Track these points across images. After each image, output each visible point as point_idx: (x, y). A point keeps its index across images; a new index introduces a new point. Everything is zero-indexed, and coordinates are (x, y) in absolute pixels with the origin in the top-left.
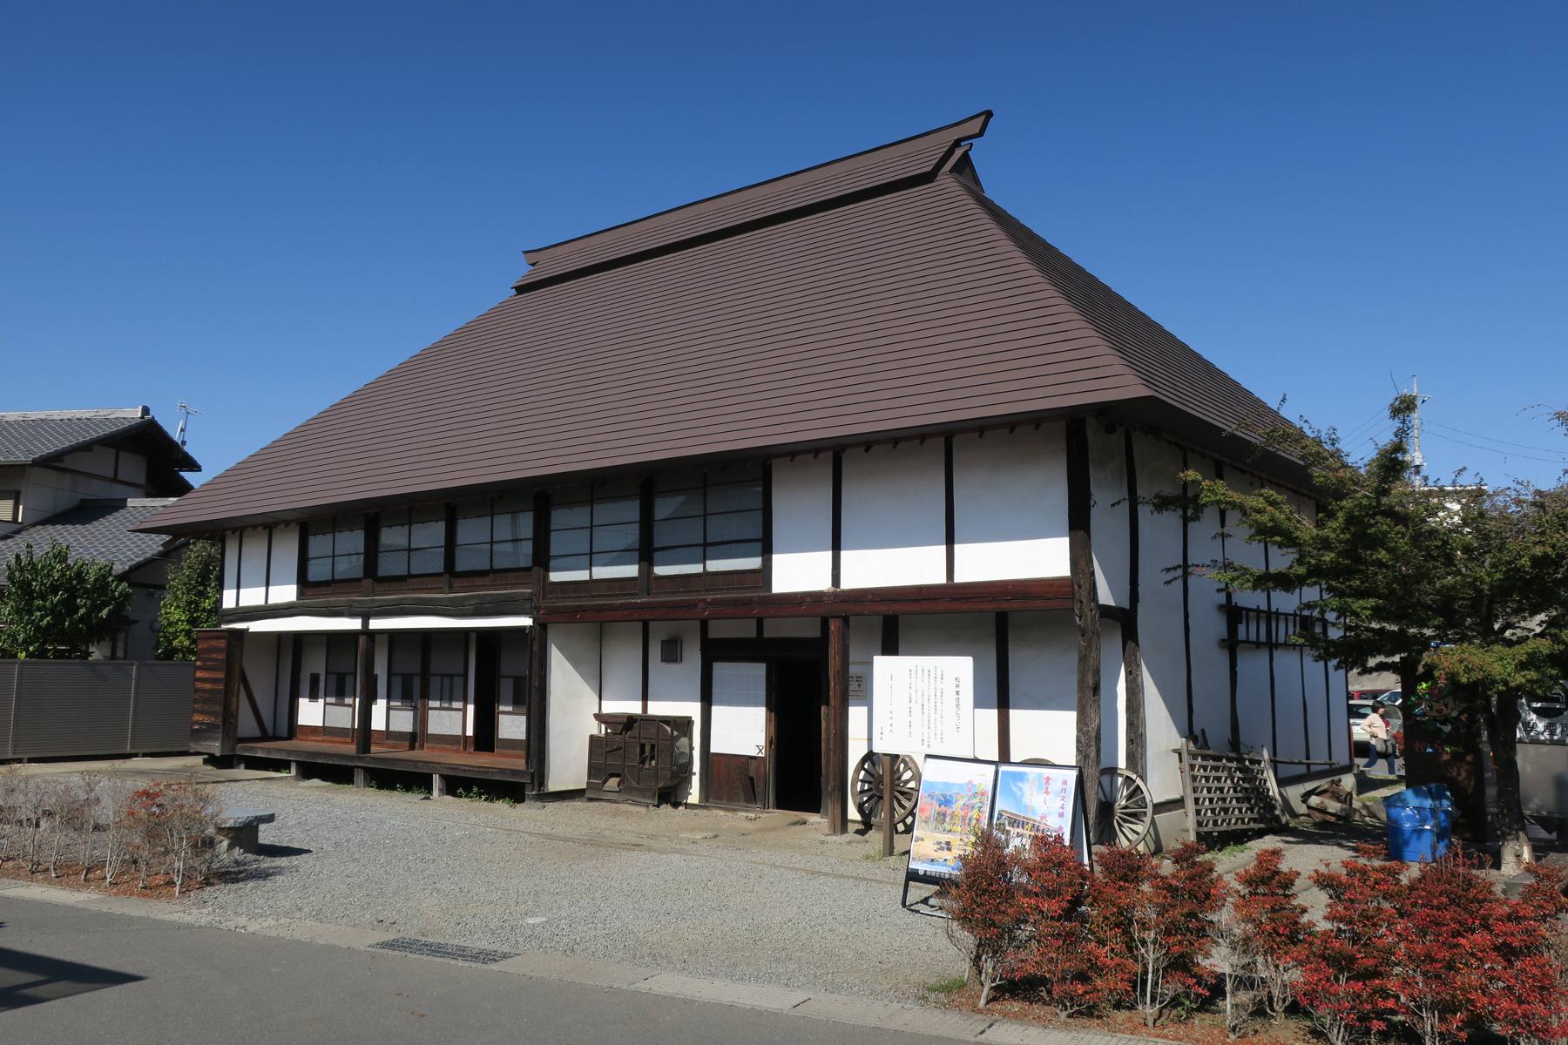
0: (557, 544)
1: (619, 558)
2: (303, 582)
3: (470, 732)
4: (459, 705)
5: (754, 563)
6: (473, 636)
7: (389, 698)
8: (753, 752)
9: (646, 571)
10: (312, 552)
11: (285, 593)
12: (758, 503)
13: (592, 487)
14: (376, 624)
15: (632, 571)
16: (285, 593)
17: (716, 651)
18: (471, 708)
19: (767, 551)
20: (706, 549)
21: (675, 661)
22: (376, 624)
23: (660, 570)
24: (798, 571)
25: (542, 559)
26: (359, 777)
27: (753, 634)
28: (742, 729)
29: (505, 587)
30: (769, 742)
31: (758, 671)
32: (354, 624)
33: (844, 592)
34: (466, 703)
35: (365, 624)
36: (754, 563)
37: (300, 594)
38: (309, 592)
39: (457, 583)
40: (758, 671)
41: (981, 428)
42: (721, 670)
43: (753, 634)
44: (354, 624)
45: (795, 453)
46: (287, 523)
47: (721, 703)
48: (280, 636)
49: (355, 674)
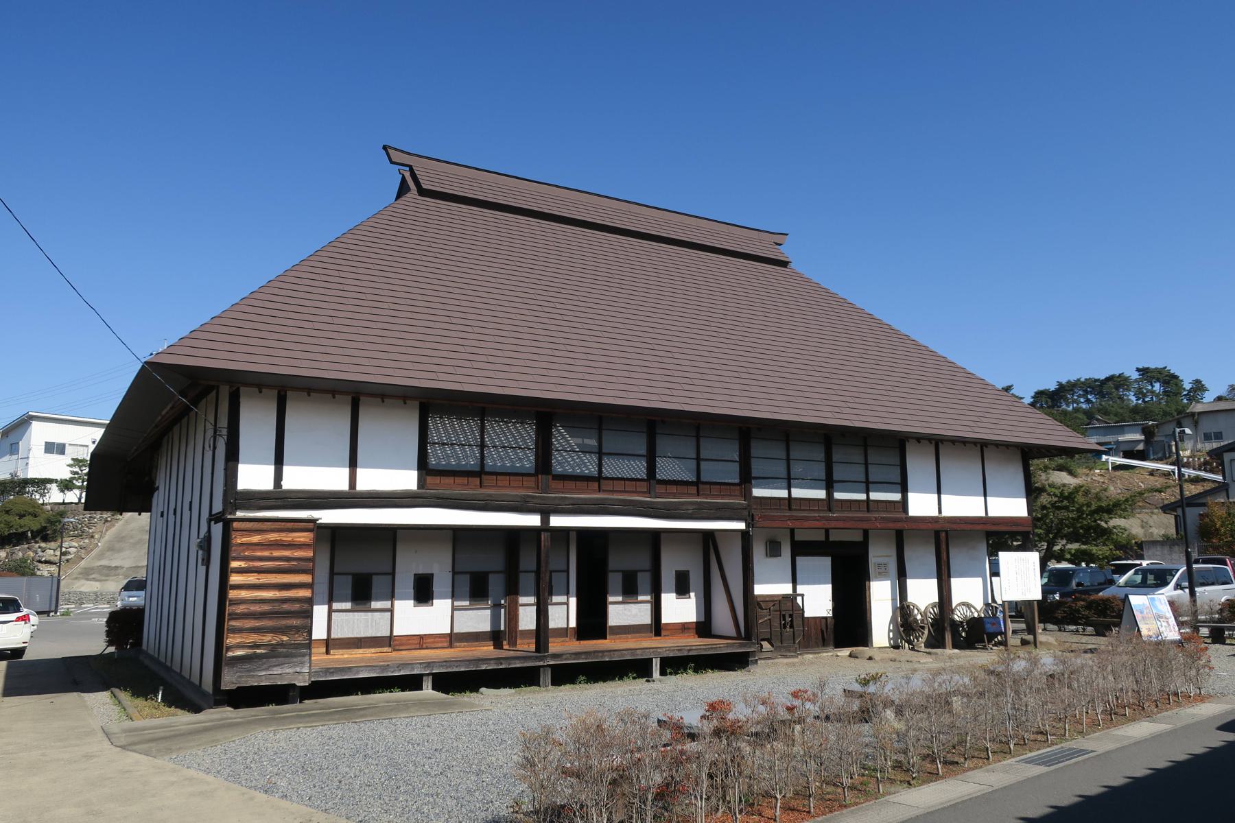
0: (757, 468)
1: (812, 483)
2: (423, 466)
3: (573, 624)
4: (563, 599)
5: (897, 497)
6: (573, 536)
7: (330, 601)
8: (825, 615)
9: (830, 495)
10: (433, 436)
11: (408, 480)
12: (897, 461)
13: (787, 434)
14: (556, 521)
15: (821, 494)
16: (408, 480)
17: (801, 549)
18: (573, 601)
19: (904, 491)
20: (867, 487)
21: (772, 556)
22: (556, 521)
23: (838, 496)
24: (921, 504)
25: (747, 479)
26: (546, 676)
27: (823, 538)
28: (818, 600)
29: (723, 496)
30: (834, 609)
31: (826, 562)
32: (534, 520)
33: (945, 518)
34: (568, 594)
35: (545, 520)
36: (897, 497)
37: (421, 483)
38: (429, 479)
39: (660, 489)
40: (826, 562)
41: (998, 445)
42: (800, 560)
43: (823, 538)
44: (534, 520)
45: (919, 438)
46: (414, 398)
47: (803, 583)
48: (583, 533)
49: (568, 571)
